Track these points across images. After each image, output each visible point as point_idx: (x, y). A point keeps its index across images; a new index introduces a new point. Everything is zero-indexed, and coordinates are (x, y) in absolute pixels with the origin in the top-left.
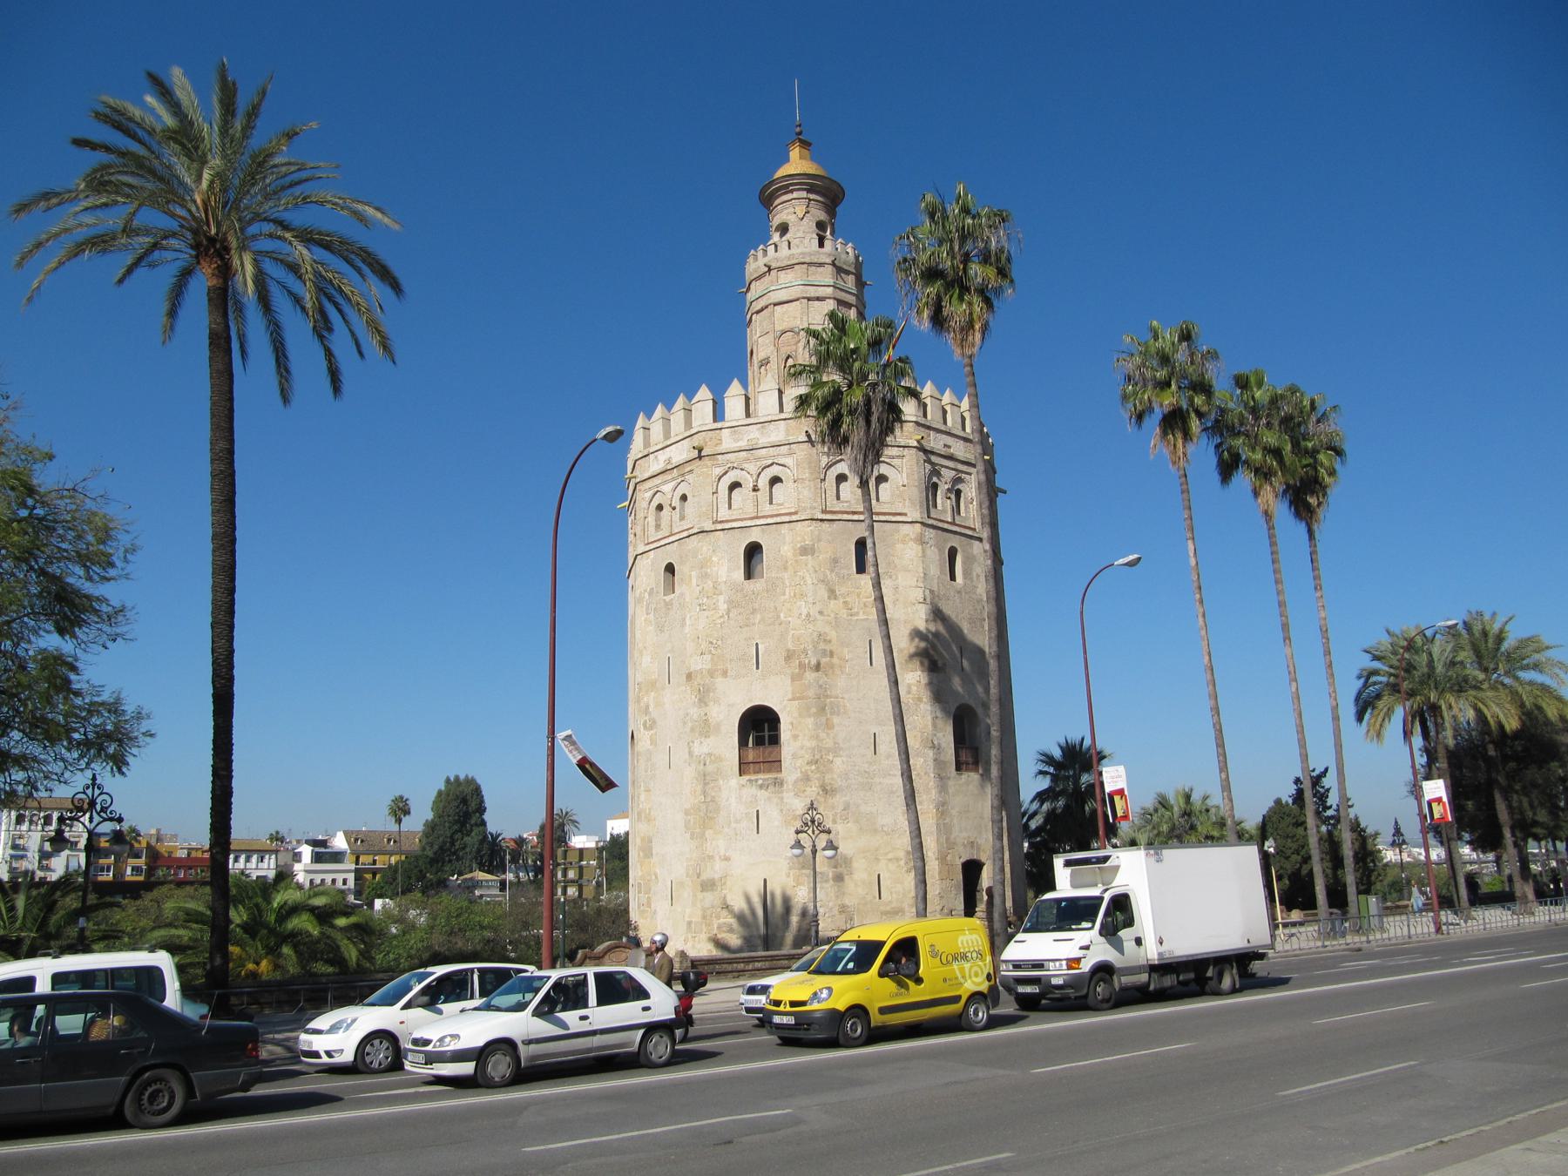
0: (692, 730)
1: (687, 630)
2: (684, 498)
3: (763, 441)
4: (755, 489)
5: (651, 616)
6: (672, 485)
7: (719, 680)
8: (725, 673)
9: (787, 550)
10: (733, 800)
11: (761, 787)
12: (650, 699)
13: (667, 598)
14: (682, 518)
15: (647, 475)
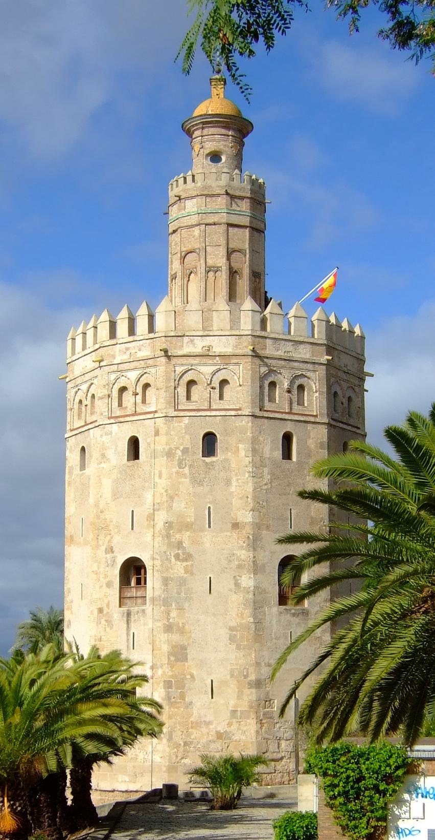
0: (239, 567)
1: (233, 489)
2: (224, 383)
3: (296, 356)
4: (289, 391)
5: (186, 470)
6: (215, 368)
7: (264, 532)
8: (268, 528)
9: (311, 444)
10: (274, 622)
11: (294, 615)
12: (186, 537)
13: (208, 460)
14: (221, 397)
15: (180, 353)
